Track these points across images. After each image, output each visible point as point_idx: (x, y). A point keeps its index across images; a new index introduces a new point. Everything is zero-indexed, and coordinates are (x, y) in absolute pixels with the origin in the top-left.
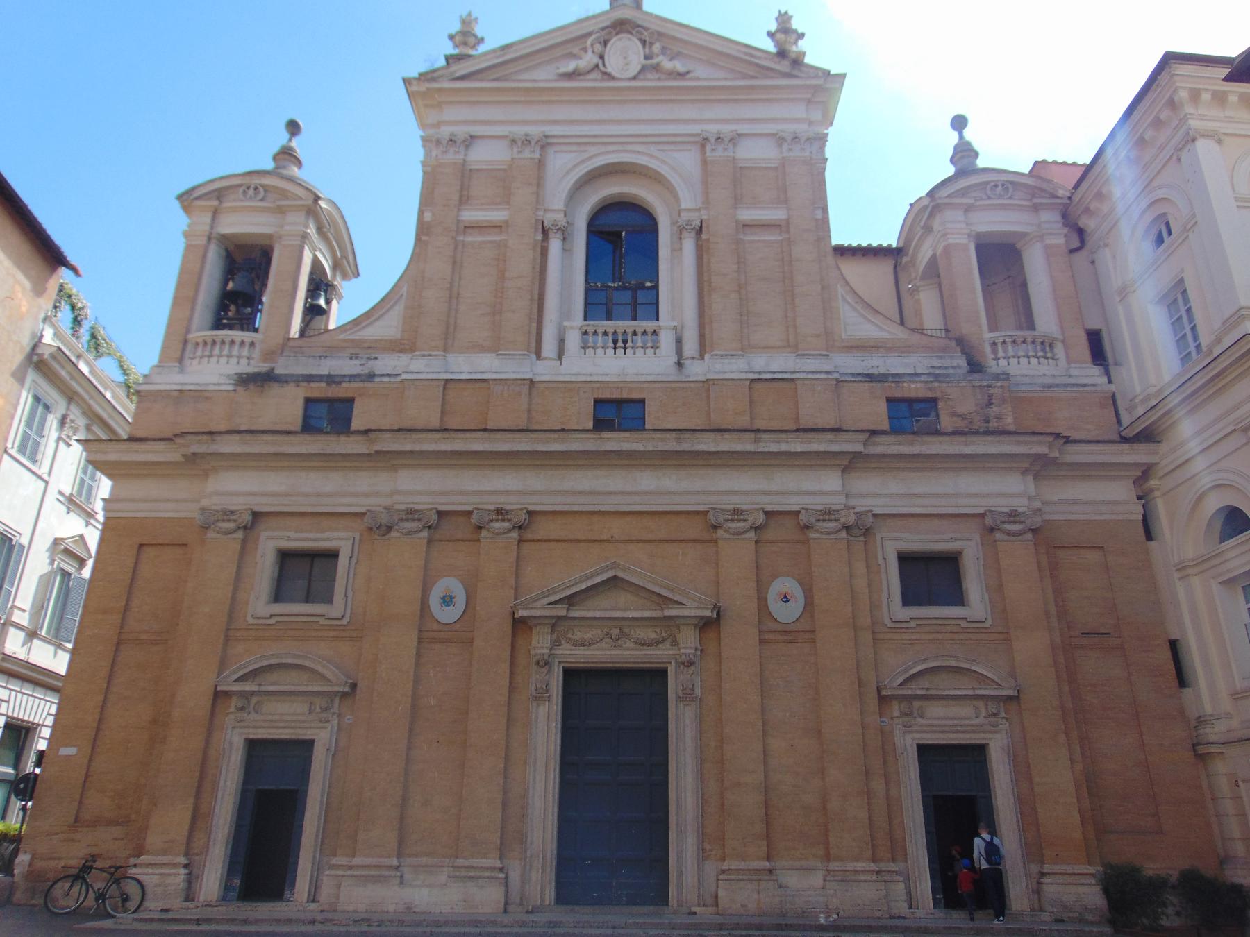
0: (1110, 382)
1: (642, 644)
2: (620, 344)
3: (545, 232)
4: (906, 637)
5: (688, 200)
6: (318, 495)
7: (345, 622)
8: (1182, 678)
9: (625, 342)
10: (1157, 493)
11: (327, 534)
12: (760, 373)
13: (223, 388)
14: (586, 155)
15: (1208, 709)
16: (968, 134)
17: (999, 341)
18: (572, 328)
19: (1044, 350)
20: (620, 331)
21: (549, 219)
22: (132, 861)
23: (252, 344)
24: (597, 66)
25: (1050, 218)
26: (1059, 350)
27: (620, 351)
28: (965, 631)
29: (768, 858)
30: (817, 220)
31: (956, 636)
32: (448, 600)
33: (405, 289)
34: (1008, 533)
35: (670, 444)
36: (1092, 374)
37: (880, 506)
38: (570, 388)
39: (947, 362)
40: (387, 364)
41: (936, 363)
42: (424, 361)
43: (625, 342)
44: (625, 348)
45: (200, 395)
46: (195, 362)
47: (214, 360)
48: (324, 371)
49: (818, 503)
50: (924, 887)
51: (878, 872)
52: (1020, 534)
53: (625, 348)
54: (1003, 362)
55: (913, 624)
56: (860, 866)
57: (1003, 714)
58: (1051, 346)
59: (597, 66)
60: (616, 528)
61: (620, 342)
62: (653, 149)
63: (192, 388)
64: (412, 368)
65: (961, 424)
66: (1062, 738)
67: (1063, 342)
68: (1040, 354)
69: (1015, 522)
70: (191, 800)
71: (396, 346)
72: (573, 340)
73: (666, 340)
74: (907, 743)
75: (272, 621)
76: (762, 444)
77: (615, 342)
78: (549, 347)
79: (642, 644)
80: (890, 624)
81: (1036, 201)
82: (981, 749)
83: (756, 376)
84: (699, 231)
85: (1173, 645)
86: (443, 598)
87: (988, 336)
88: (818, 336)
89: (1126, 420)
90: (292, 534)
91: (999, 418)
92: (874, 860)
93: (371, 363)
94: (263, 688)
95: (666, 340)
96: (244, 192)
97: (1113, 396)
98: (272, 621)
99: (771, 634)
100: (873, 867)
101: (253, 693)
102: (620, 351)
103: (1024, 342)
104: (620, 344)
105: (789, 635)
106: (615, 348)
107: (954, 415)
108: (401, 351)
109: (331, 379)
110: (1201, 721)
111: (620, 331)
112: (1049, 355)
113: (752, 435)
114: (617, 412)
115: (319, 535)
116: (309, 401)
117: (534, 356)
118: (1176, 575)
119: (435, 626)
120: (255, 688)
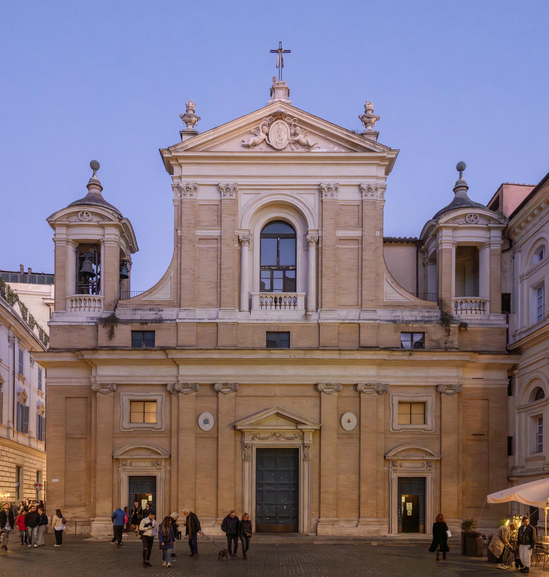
0: (507, 323)
1: (288, 439)
2: (278, 303)
3: (240, 242)
4: (398, 436)
5: (312, 225)
6: (144, 377)
7: (162, 430)
8: (510, 451)
9: (280, 303)
10: (516, 376)
11: (150, 394)
12: (344, 320)
13: (90, 324)
14: (259, 196)
15: (517, 464)
16: (466, 177)
17: (459, 301)
18: (255, 295)
19: (480, 307)
20: (278, 297)
21: (242, 234)
22: (92, 519)
23: (99, 300)
24: (265, 140)
25: (496, 234)
26: (488, 305)
27: (278, 307)
28: (423, 434)
29: (337, 517)
30: (376, 237)
31: (419, 436)
32: (206, 422)
33: (172, 274)
34: (447, 394)
35: (300, 355)
36: (499, 320)
37: (392, 382)
38: (254, 326)
39: (432, 314)
40: (168, 313)
41: (427, 314)
42: (186, 312)
43: (280, 303)
44: (280, 306)
45: (78, 327)
46: (73, 310)
47: (82, 309)
48: (138, 317)
49: (366, 381)
50: (395, 526)
51: (378, 522)
52: (452, 394)
53: (280, 306)
54: (459, 312)
55: (402, 431)
56: (371, 519)
57: (434, 466)
58: (484, 304)
59: (265, 140)
60: (278, 391)
61: (277, 302)
62: (294, 193)
63: (75, 324)
64: (180, 317)
65: (434, 344)
66: (456, 475)
67: (490, 302)
68: (478, 308)
69: (451, 390)
70: (111, 498)
71: (170, 304)
72: (256, 301)
73: (301, 302)
74: (395, 476)
75: (132, 430)
76: (342, 355)
77: (276, 302)
78: (245, 305)
79: (288, 439)
80: (391, 430)
81: (489, 225)
82: (424, 479)
83: (341, 321)
84: (317, 243)
85: (510, 440)
86: (205, 421)
87: (454, 298)
88: (372, 301)
89: (511, 341)
90: (135, 394)
91: (452, 342)
92: (377, 517)
93: (160, 313)
94: (133, 457)
95: (301, 302)
96: (82, 215)
97: (507, 330)
98: (132, 430)
99: (342, 434)
100: (376, 520)
101: (128, 459)
102: (278, 307)
103: (471, 302)
104: (278, 303)
105: (349, 435)
106: (276, 306)
107: (431, 340)
108: (173, 307)
109: (144, 322)
110: (514, 468)
111: (278, 297)
112: (482, 309)
113: (338, 352)
114: (278, 339)
115: (148, 394)
116: (133, 332)
117: (237, 310)
118: (517, 411)
119: (202, 432)
120: (129, 457)
